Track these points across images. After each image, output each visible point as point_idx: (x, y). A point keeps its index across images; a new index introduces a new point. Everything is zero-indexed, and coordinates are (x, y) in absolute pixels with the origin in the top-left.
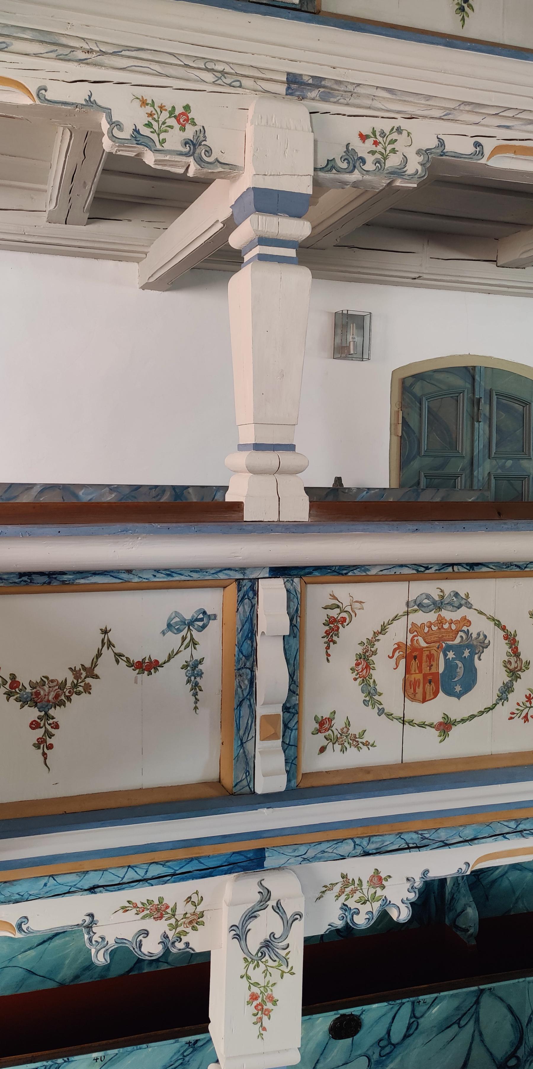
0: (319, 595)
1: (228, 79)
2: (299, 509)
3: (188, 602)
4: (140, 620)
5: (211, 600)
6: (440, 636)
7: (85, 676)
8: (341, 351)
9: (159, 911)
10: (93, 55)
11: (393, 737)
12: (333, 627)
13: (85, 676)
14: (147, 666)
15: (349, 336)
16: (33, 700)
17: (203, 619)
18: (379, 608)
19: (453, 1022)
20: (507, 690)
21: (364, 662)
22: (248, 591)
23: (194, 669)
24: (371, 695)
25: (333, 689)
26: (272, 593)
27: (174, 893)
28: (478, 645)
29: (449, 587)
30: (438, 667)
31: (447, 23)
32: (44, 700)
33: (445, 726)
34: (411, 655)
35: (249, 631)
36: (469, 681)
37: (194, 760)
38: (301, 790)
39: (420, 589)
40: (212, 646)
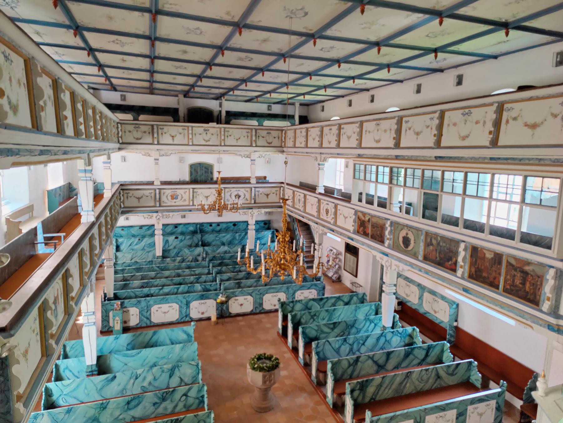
0: (162, 191)
1: (152, 150)
2: (159, 184)
3: (150, 191)
5: (153, 191)
6: (174, 194)
7: (142, 197)
10: (140, 149)
12: (164, 194)
13: (142, 197)
19: (190, 239)
21: (167, 196)
22: (155, 190)
24: (168, 199)
25: (164, 198)
26: (157, 191)
27: (151, 214)
28: (178, 195)
30: (174, 197)
31: (172, 143)
32: (139, 199)
34: (172, 196)
37: (153, 204)
38: (160, 206)
40: (153, 195)
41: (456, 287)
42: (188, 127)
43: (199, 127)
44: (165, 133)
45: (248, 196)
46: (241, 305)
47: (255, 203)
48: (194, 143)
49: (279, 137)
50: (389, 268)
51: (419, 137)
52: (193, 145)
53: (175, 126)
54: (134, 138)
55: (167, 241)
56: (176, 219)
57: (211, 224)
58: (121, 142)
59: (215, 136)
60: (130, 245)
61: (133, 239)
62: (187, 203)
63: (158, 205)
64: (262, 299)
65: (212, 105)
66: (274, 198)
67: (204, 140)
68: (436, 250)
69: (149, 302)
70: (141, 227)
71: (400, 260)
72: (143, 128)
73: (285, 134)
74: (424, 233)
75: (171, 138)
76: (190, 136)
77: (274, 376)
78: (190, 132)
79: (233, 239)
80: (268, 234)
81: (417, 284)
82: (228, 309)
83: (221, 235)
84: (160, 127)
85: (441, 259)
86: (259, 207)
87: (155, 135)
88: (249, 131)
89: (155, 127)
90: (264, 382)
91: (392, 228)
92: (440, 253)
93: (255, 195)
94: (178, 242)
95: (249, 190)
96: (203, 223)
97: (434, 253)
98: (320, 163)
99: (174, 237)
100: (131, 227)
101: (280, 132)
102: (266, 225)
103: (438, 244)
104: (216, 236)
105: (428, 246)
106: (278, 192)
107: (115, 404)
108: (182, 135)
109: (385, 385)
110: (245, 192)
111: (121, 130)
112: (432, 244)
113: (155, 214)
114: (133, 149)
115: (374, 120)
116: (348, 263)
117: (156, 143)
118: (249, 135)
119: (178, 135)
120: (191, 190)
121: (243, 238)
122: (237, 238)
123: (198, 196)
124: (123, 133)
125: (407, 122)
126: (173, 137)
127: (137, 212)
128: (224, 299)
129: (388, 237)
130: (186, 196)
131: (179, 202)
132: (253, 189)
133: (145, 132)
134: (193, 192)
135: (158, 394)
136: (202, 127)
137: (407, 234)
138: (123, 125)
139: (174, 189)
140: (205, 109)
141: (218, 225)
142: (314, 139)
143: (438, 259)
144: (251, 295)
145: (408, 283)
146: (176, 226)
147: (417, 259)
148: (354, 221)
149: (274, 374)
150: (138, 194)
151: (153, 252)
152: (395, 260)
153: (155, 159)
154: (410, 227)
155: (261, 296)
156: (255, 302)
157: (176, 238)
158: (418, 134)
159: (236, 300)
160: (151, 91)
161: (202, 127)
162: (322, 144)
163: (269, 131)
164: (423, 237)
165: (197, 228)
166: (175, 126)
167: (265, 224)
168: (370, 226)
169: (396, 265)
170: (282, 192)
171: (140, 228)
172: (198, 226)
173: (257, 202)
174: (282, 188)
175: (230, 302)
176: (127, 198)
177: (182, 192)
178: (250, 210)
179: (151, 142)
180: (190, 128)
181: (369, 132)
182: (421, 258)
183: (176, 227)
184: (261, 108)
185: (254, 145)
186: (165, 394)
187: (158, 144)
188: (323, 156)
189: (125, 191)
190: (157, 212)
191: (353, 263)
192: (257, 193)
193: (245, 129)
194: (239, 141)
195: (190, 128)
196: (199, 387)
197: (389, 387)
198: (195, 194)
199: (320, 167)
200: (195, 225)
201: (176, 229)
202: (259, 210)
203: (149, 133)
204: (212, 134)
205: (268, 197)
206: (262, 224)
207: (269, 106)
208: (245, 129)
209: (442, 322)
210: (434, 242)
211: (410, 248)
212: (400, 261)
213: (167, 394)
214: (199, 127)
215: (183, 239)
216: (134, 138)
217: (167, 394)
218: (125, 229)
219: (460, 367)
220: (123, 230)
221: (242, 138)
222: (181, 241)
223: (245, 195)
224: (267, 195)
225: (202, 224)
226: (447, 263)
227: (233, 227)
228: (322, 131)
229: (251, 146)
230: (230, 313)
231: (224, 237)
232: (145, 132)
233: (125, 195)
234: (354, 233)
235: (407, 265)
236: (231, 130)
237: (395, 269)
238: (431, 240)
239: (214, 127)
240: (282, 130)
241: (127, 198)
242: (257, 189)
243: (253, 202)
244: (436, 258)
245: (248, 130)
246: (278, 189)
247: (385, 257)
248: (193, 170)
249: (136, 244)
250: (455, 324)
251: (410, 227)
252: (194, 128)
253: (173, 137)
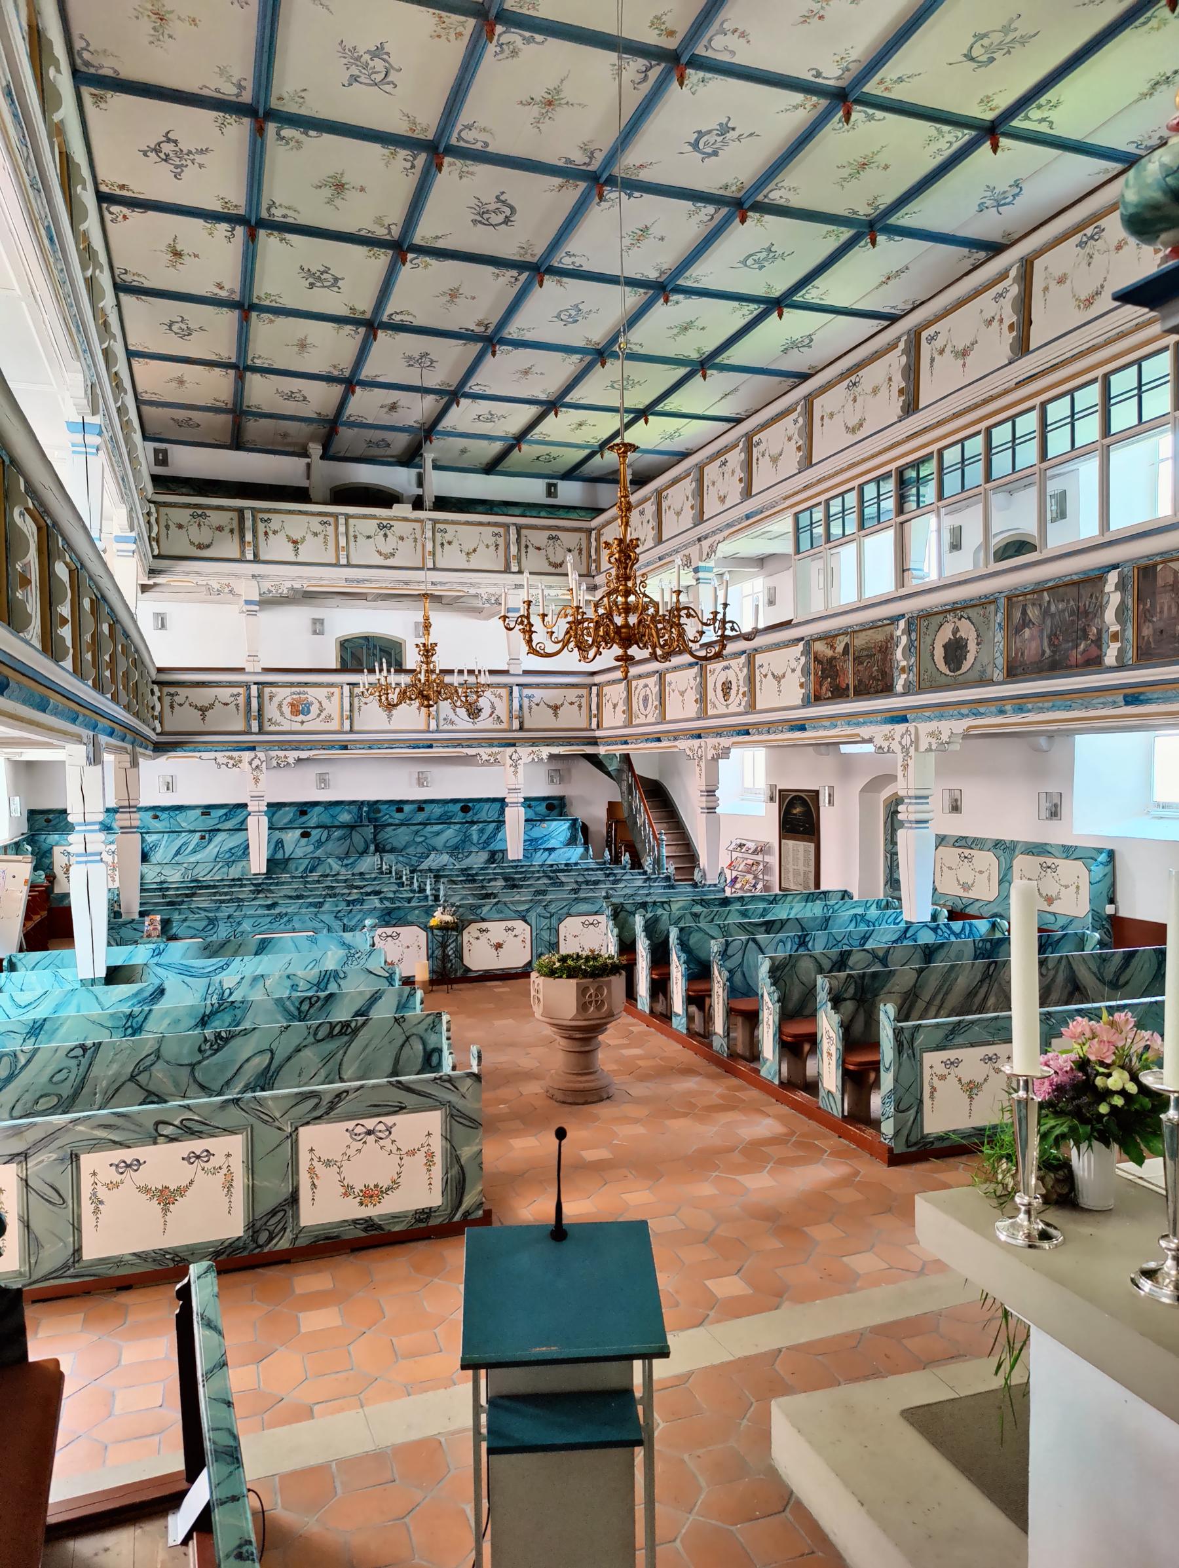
0: (267, 690)
1: (238, 577)
3: (235, 690)
4: (225, 694)
5: (241, 690)
6: (300, 701)
7: (212, 705)
8: (315, 633)
9: (231, 758)
11: (289, 722)
12: (271, 698)
13: (212, 705)
14: (227, 704)
15: (318, 627)
16: (200, 710)
17: (239, 694)
18: (282, 693)
20: (319, 715)
21: (280, 706)
22: (249, 688)
23: (237, 705)
24: (282, 714)
25: (271, 711)
26: (254, 688)
27: (235, 754)
29: (302, 689)
30: (299, 708)
31: (293, 559)
32: (203, 710)
33: (302, 723)
34: (292, 705)
35: (249, 697)
36: (309, 712)
37: (240, 726)
38: (261, 731)
39: (294, 689)
40: (241, 700)
41: (1105, 705)
42: (336, 516)
43: (365, 517)
44: (275, 532)
45: (502, 710)
46: (498, 946)
47: (521, 729)
48: (353, 562)
49: (580, 550)
50: (912, 749)
51: (968, 359)
52: (348, 565)
53: (301, 512)
54: (192, 543)
55: (279, 844)
56: (300, 787)
57: (399, 805)
58: (156, 552)
59: (409, 543)
60: (178, 853)
61: (184, 837)
62: (334, 725)
63: (255, 728)
64: (557, 931)
65: (399, 478)
66: (572, 718)
67: (380, 553)
69: (239, 924)
70: (207, 810)
71: (941, 711)
72: (215, 518)
73: (598, 540)
75: (291, 545)
76: (342, 542)
77: (609, 992)
78: (342, 529)
79: (464, 841)
80: (559, 830)
81: (990, 845)
82: (461, 959)
83: (429, 828)
84: (261, 515)
86: (534, 742)
87: (249, 537)
88: (501, 530)
89: (248, 514)
90: (583, 1007)
91: (913, 636)
93: (521, 707)
94: (311, 848)
95: (504, 692)
96: (378, 801)
98: (701, 564)
99: (298, 832)
100: (180, 808)
101: (583, 536)
102: (556, 806)
103: (1046, 613)
104: (417, 833)
105: (1018, 630)
106: (584, 701)
107: (167, 1021)
108: (321, 537)
109: (926, 997)
110: (493, 698)
111: (157, 519)
113: (247, 756)
114: (187, 574)
115: (843, 376)
116: (789, 866)
117: (250, 557)
118: (501, 541)
119: (309, 537)
120: (346, 688)
121: (493, 836)
122: (475, 838)
123: (364, 707)
124: (163, 531)
125: (931, 339)
126: (295, 542)
127: (196, 747)
128: (448, 918)
129: (904, 663)
130: (332, 707)
131: (313, 723)
132: (516, 689)
133: (220, 529)
134: (351, 695)
135: (288, 1003)
136: (374, 517)
137: (956, 631)
138: (163, 510)
139: (299, 685)
140: (379, 491)
141: (421, 809)
142: (678, 514)
144: (526, 921)
145: (967, 852)
146: (304, 808)
147: (991, 682)
148: (806, 672)
149: (609, 984)
150: (203, 696)
151: (244, 863)
152: (929, 719)
153: (248, 602)
154: (962, 609)
155: (554, 921)
156: (536, 940)
157: (305, 835)
158: (965, 353)
159: (482, 931)
160: (237, 442)
161: (374, 517)
162: (702, 512)
163: (554, 533)
165: (361, 817)
166: (301, 512)
167: (550, 807)
168: (849, 665)
169: (931, 734)
170: (595, 700)
171: (203, 814)
172: (365, 809)
173: (526, 726)
174: (594, 689)
175: (469, 935)
176: (172, 707)
177: (321, 693)
178: (510, 750)
179: (237, 555)
180: (342, 520)
181: (832, 415)
182: (998, 675)
183: (303, 813)
184: (532, 490)
185: (515, 568)
186: (305, 1007)
187: (256, 559)
188: (706, 544)
189: (166, 690)
190: (253, 749)
191: (806, 859)
192: (526, 701)
193: (489, 524)
194: (473, 557)
195: (342, 520)
196: (400, 996)
197: (937, 1002)
198: (356, 700)
199: (701, 575)
200: (354, 808)
201: (305, 818)
202: (535, 749)
203: (232, 531)
204: (402, 538)
205: (556, 715)
206: (542, 808)
207: (549, 486)
208: (489, 524)
209: (1072, 920)
211: (966, 666)
212: (941, 717)
213: (311, 1005)
214: (365, 517)
215: (323, 839)
216: (192, 543)
217: (311, 1005)
218: (163, 815)
219: (1135, 962)
220: (156, 817)
221: (481, 548)
222: (319, 844)
223: (493, 707)
224: (556, 708)
225: (374, 805)
227: (461, 814)
228: (700, 481)
229: (507, 570)
230: (468, 970)
231: (438, 834)
232: (220, 529)
233: (167, 700)
234: (807, 702)
235: (964, 716)
236: (451, 528)
237: (929, 750)
238: (1024, 613)
239: (406, 519)
240: (589, 531)
241: (172, 707)
242: (527, 692)
243: (516, 724)
244: (1044, 652)
245: (496, 530)
246: (584, 692)
247: (900, 728)
248: (348, 658)
249: (194, 851)
250: (1110, 909)
252: (351, 521)
253: (295, 542)
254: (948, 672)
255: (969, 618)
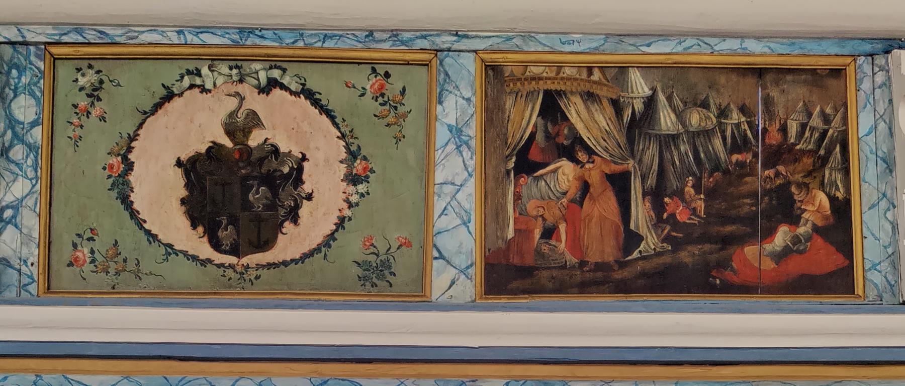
68: (619, 183)
74: (466, 71)
85: (679, 237)
92: (656, 196)
97: (609, 204)
103: (639, 125)
105: (526, 165)
112: (572, 148)
143: (651, 242)
164: (459, 108)
210: (588, 121)
226: (750, 251)
251: (274, 62)
254: (205, 250)
255: (309, 94)
